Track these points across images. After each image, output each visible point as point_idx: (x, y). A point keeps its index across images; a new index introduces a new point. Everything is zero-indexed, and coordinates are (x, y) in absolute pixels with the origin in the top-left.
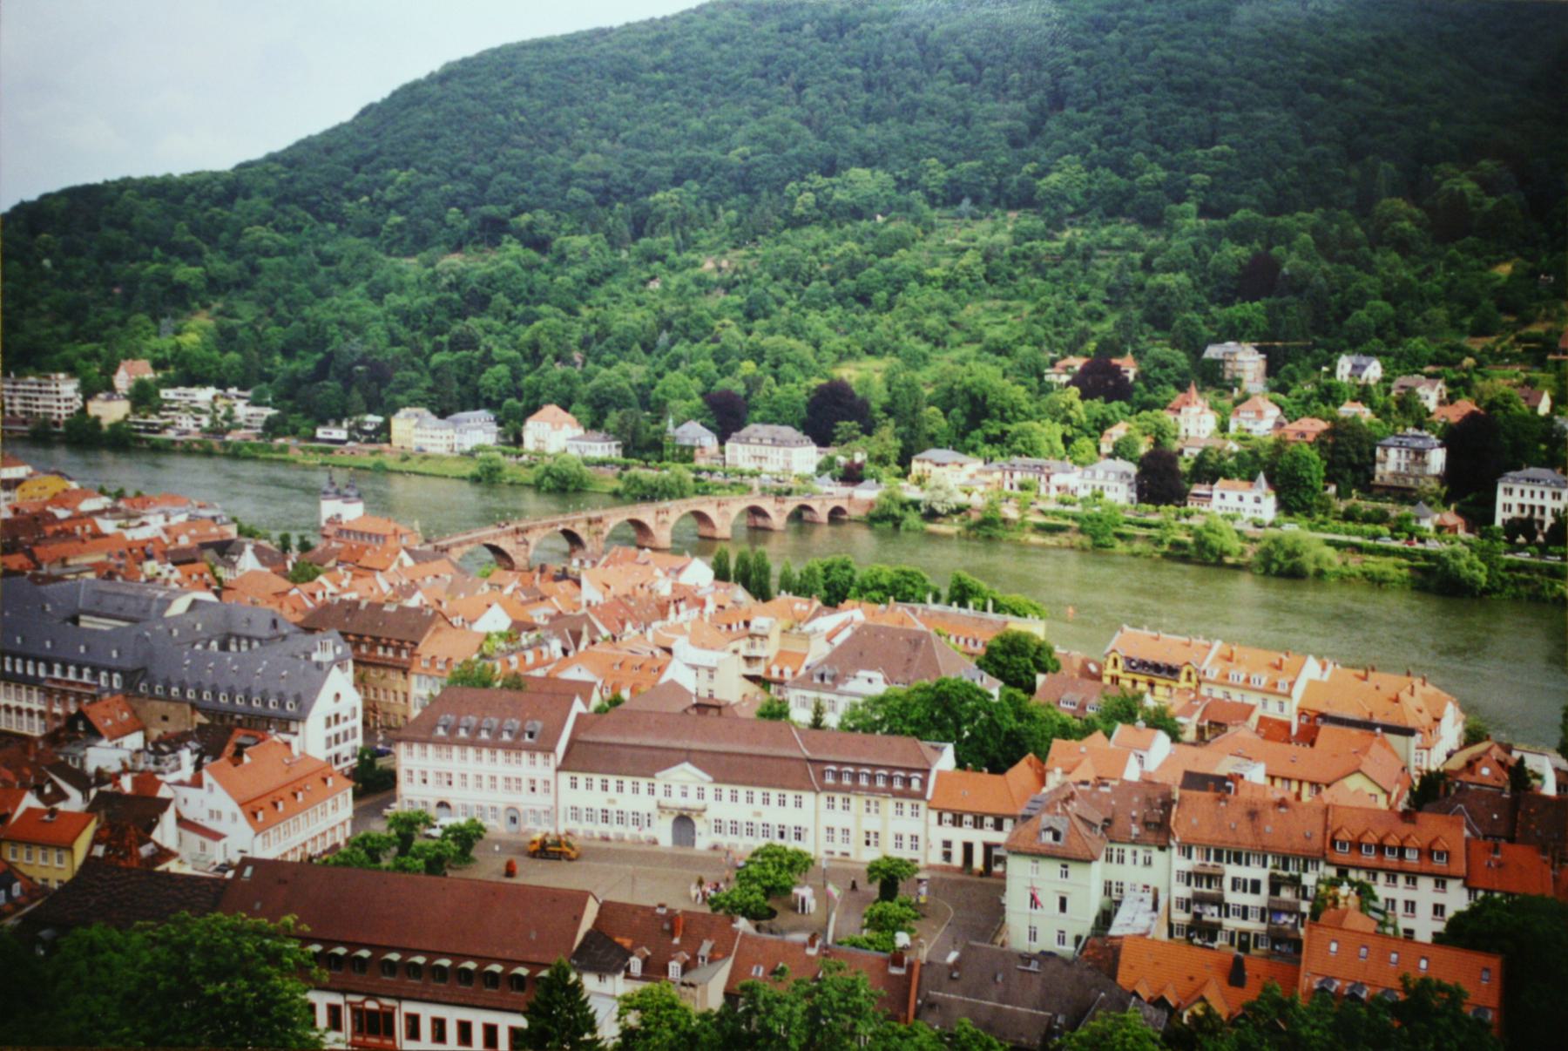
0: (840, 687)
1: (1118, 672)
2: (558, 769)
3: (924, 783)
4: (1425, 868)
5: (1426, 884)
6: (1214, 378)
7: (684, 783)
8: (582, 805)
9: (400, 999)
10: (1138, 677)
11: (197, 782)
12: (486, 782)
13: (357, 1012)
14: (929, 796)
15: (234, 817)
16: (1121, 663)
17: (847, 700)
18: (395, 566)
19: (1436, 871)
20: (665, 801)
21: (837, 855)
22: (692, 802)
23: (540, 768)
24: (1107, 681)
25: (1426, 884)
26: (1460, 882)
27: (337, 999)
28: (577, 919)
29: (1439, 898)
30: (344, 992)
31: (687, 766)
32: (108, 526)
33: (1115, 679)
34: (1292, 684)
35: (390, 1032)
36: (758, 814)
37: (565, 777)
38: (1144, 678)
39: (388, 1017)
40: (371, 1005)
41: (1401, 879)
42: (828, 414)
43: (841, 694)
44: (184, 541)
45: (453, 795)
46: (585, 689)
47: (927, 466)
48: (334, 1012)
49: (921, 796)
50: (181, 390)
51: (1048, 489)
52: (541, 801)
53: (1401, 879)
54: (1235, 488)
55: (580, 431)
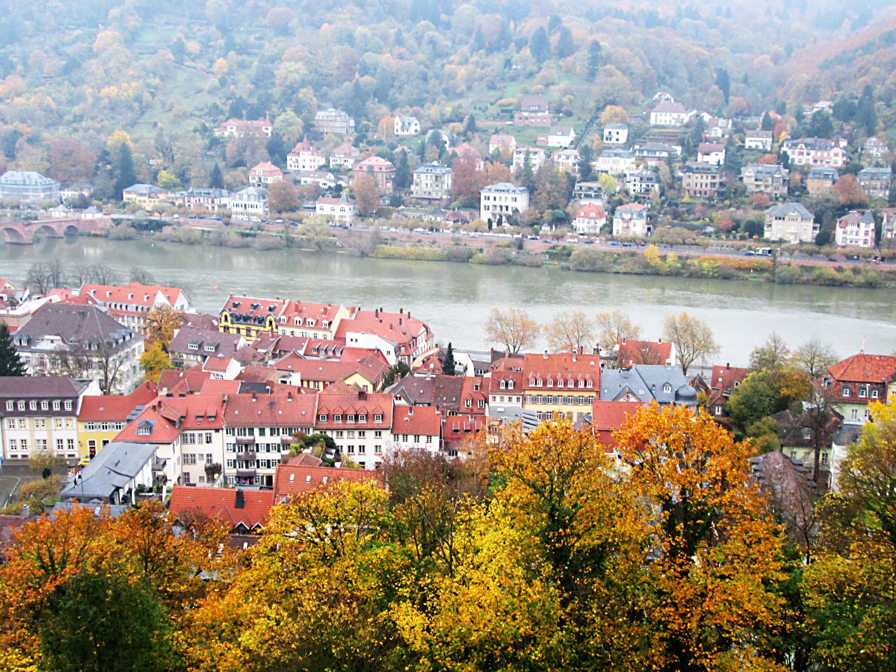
0: (33, 348)
1: (229, 324)
3: (74, 405)
4: (369, 426)
5: (370, 434)
6: (312, 135)
10: (241, 326)
14: (78, 413)
16: (229, 319)
17: (37, 355)
19: (376, 427)
21: (20, 457)
24: (222, 330)
25: (370, 434)
26: (389, 431)
29: (378, 442)
33: (226, 328)
34: (330, 323)
38: (244, 327)
41: (356, 433)
43: (33, 352)
47: (133, 196)
49: (72, 414)
51: (213, 208)
53: (345, 433)
54: (329, 203)
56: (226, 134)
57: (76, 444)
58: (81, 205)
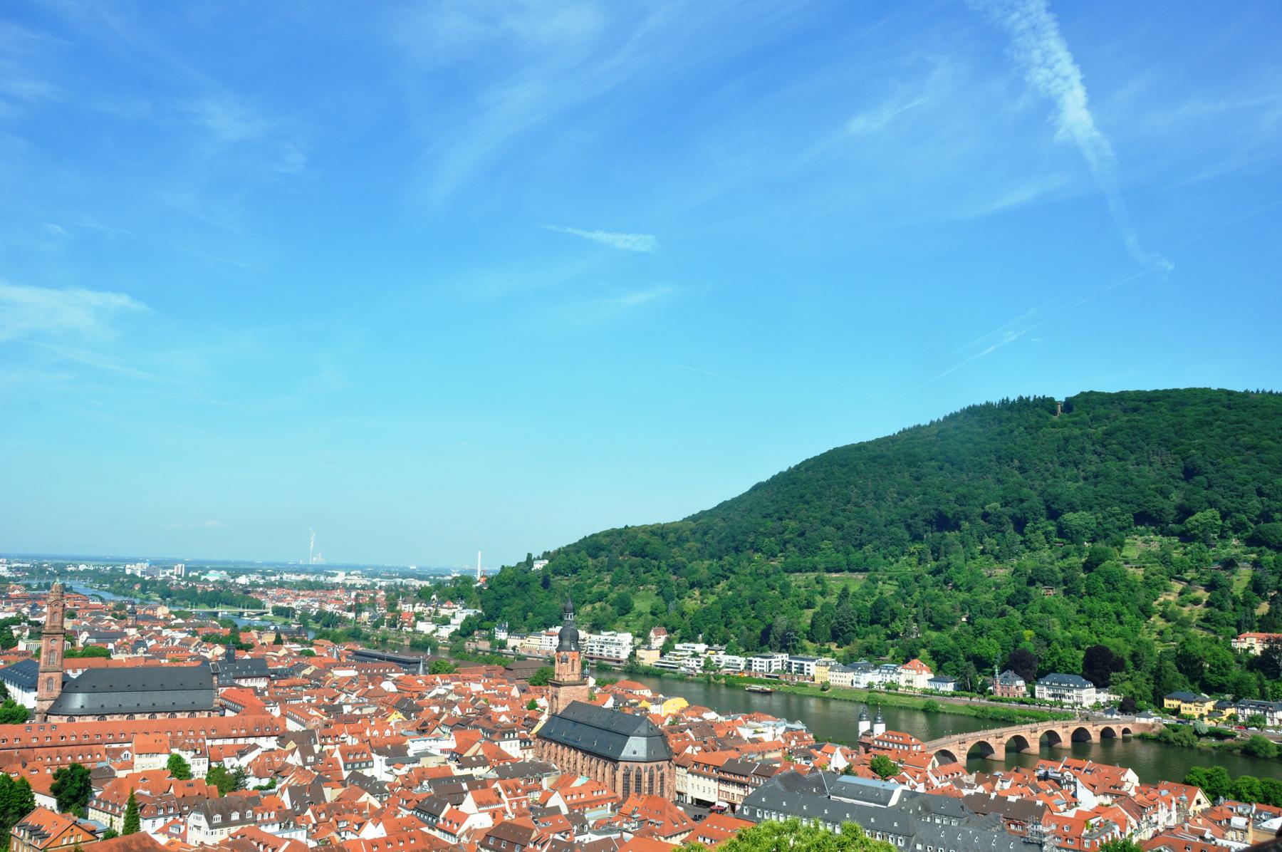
42: (1099, 668)
55: (932, 676)
56: (1245, 646)
58: (1127, 707)
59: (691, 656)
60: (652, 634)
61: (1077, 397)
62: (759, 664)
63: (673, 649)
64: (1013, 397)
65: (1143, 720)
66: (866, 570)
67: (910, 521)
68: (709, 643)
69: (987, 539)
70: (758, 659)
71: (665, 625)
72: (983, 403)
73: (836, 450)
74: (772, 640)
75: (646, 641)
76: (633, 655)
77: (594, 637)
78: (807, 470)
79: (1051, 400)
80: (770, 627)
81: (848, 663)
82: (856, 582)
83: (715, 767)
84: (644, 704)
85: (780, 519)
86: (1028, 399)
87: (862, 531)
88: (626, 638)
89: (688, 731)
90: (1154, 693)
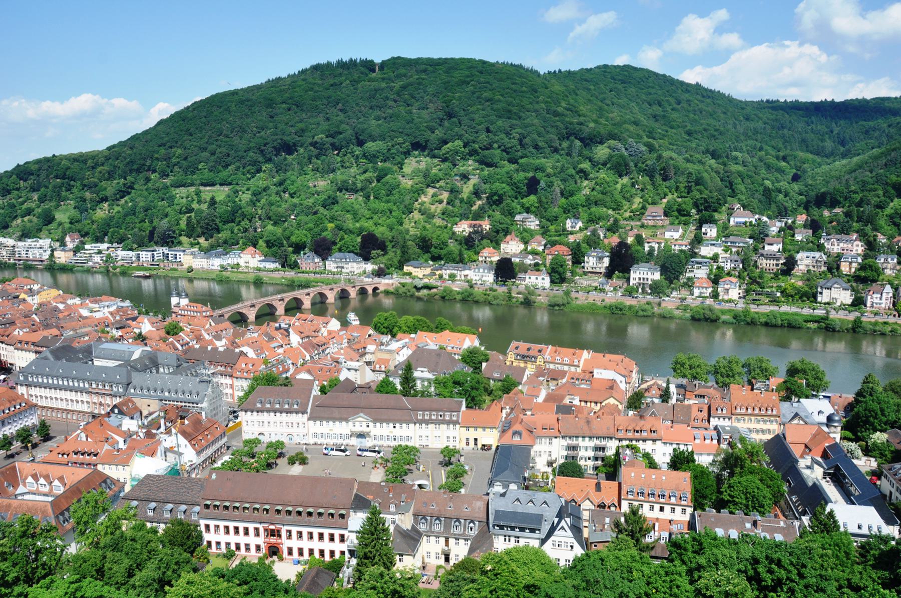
2: (309, 419)
7: (360, 423)
8: (319, 432)
9: (283, 525)
11: (168, 432)
12: (278, 424)
13: (266, 530)
15: (186, 446)
18: (208, 326)
20: (354, 429)
22: (364, 429)
23: (302, 418)
27: (257, 525)
28: (352, 489)
30: (261, 523)
31: (362, 414)
32: (85, 313)
35: (279, 536)
36: (391, 432)
37: (311, 422)
39: (279, 531)
40: (272, 527)
42: (369, 247)
44: (118, 318)
45: (265, 429)
46: (310, 383)
48: (257, 529)
50: (93, 245)
52: (302, 431)
57: (458, 440)
58: (380, 273)
59: (96, 253)
60: (68, 239)
61: (389, 60)
62: (146, 256)
63: (83, 249)
64: (346, 59)
65: (387, 281)
66: (230, 184)
67: (263, 148)
68: (111, 242)
69: (314, 160)
70: (144, 253)
71: (79, 232)
72: (325, 62)
73: (217, 95)
74: (156, 238)
75: (63, 244)
76: (52, 255)
77: (20, 244)
78: (194, 110)
79: (372, 61)
80: (154, 228)
81: (207, 252)
82: (221, 193)
83: (33, 344)
84: (22, 296)
85: (171, 147)
86: (355, 60)
87: (228, 155)
88: (45, 242)
89: (34, 316)
90: (400, 262)
